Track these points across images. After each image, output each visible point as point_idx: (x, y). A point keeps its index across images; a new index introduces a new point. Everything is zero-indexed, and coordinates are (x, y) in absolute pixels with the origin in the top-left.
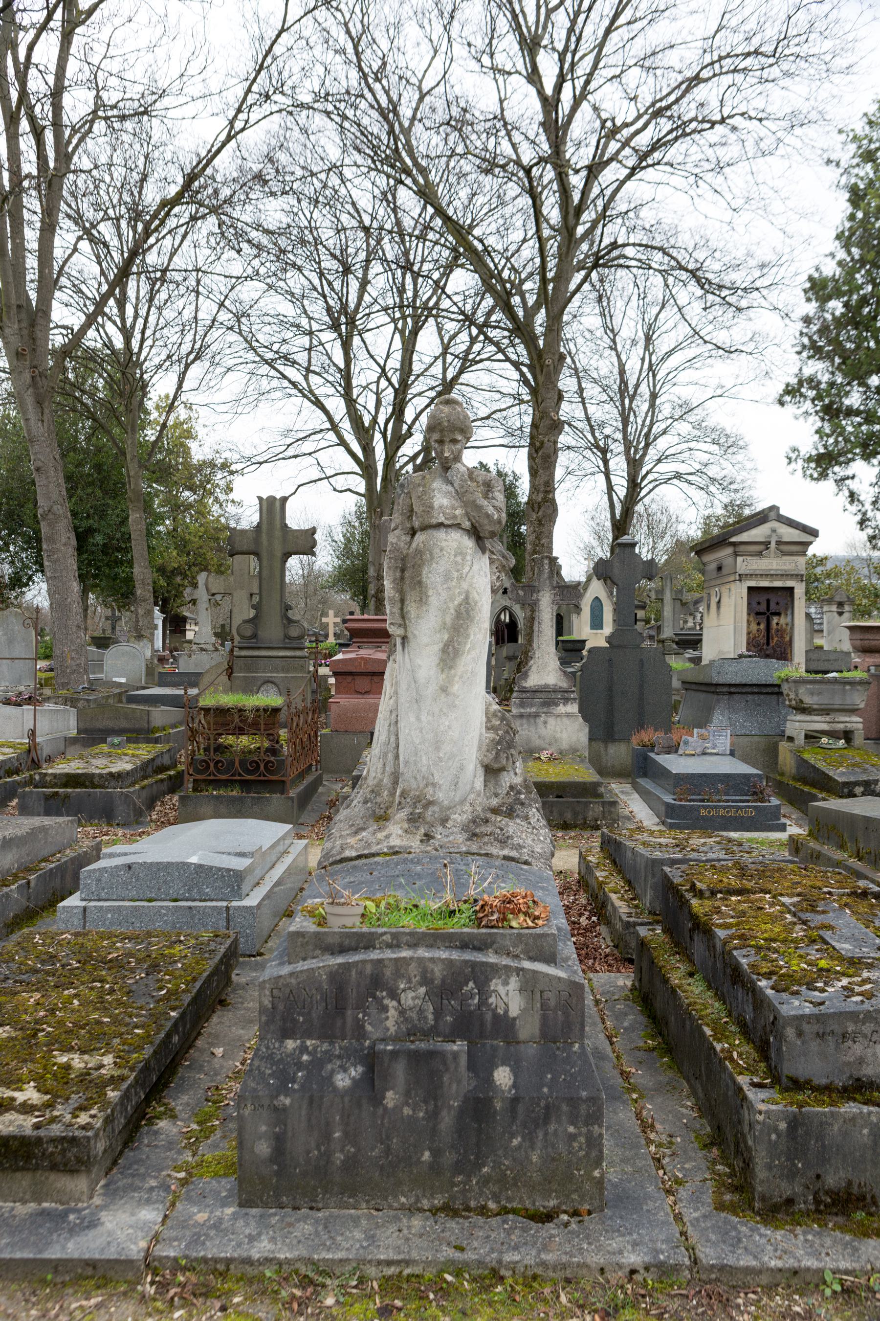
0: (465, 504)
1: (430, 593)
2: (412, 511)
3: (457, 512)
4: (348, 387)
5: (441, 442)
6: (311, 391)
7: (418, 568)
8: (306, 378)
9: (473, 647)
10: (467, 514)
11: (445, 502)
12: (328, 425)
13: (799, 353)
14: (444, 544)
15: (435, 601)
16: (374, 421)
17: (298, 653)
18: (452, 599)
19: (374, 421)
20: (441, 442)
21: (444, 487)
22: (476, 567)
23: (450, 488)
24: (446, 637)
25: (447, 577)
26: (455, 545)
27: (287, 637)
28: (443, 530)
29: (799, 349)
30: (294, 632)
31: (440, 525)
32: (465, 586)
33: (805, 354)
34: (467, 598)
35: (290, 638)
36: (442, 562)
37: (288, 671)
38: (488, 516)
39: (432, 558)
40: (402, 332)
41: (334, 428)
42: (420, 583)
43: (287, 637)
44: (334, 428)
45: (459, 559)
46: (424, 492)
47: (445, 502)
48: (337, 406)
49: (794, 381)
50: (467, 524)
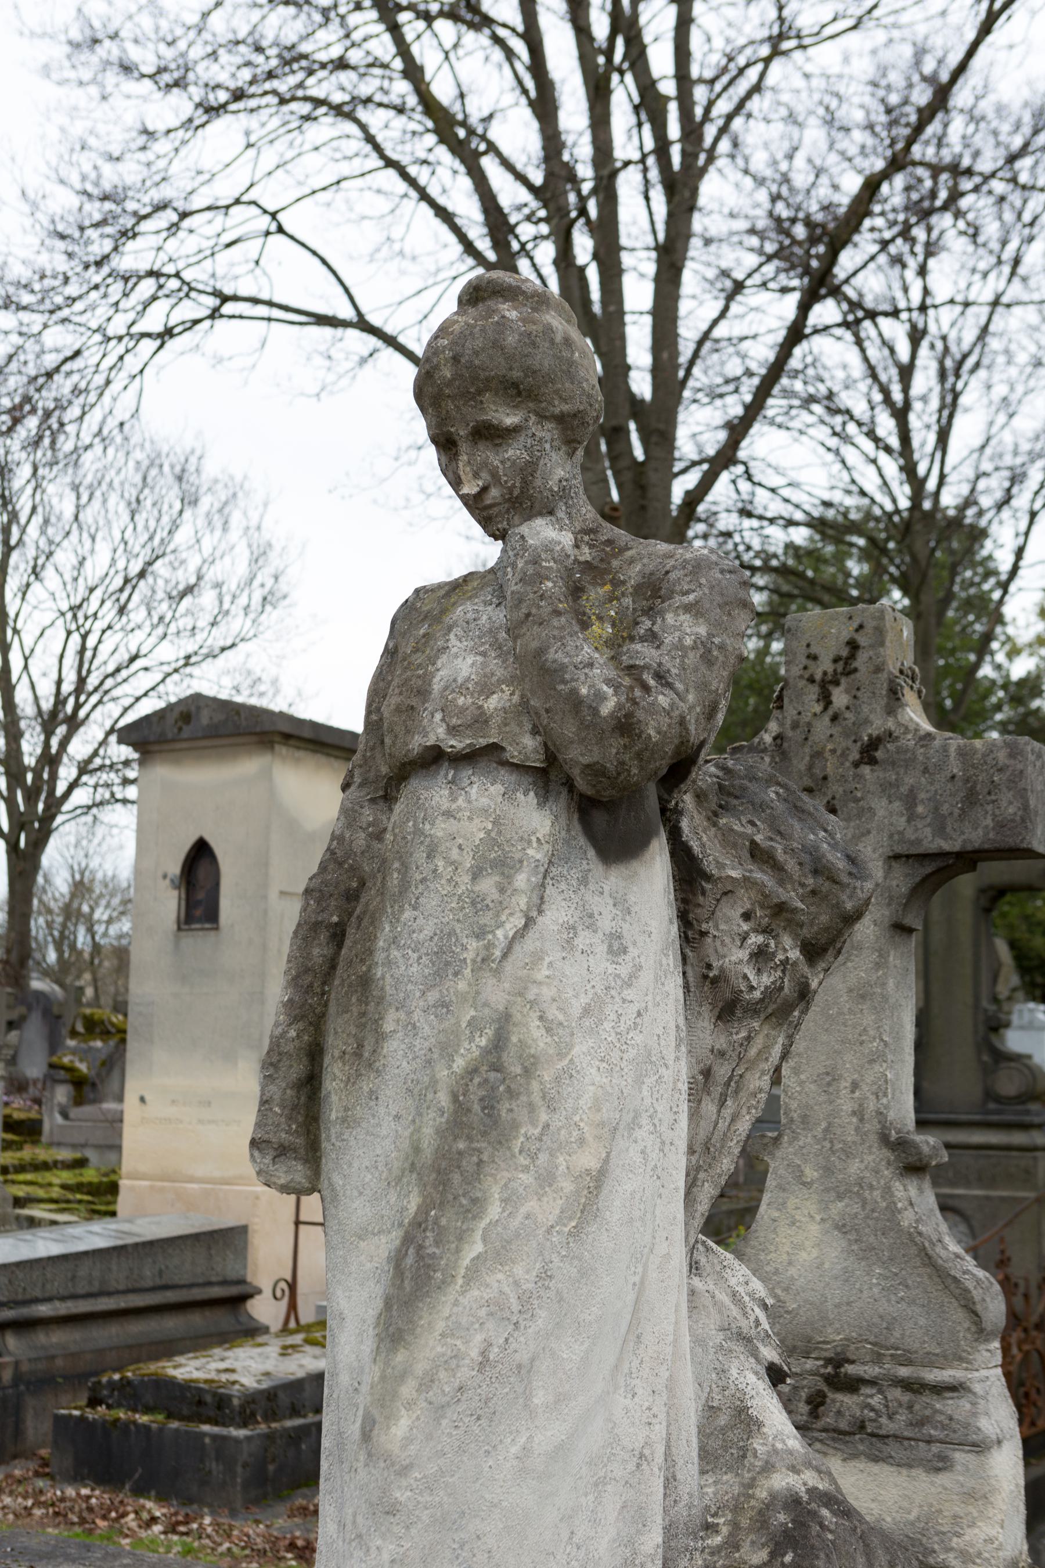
9: (500, 1253)
15: (399, 1054)
17: (1018, 1138)
18: (447, 1049)
22: (557, 914)
24: (413, 1203)
26: (476, 830)
27: (990, 1095)
30: (1008, 1085)
31: (434, 758)
32: (496, 994)
34: (499, 1043)
35: (999, 1099)
36: (430, 902)
37: (991, 1183)
39: (405, 885)
43: (990, 1095)
45: (488, 885)
50: (526, 746)
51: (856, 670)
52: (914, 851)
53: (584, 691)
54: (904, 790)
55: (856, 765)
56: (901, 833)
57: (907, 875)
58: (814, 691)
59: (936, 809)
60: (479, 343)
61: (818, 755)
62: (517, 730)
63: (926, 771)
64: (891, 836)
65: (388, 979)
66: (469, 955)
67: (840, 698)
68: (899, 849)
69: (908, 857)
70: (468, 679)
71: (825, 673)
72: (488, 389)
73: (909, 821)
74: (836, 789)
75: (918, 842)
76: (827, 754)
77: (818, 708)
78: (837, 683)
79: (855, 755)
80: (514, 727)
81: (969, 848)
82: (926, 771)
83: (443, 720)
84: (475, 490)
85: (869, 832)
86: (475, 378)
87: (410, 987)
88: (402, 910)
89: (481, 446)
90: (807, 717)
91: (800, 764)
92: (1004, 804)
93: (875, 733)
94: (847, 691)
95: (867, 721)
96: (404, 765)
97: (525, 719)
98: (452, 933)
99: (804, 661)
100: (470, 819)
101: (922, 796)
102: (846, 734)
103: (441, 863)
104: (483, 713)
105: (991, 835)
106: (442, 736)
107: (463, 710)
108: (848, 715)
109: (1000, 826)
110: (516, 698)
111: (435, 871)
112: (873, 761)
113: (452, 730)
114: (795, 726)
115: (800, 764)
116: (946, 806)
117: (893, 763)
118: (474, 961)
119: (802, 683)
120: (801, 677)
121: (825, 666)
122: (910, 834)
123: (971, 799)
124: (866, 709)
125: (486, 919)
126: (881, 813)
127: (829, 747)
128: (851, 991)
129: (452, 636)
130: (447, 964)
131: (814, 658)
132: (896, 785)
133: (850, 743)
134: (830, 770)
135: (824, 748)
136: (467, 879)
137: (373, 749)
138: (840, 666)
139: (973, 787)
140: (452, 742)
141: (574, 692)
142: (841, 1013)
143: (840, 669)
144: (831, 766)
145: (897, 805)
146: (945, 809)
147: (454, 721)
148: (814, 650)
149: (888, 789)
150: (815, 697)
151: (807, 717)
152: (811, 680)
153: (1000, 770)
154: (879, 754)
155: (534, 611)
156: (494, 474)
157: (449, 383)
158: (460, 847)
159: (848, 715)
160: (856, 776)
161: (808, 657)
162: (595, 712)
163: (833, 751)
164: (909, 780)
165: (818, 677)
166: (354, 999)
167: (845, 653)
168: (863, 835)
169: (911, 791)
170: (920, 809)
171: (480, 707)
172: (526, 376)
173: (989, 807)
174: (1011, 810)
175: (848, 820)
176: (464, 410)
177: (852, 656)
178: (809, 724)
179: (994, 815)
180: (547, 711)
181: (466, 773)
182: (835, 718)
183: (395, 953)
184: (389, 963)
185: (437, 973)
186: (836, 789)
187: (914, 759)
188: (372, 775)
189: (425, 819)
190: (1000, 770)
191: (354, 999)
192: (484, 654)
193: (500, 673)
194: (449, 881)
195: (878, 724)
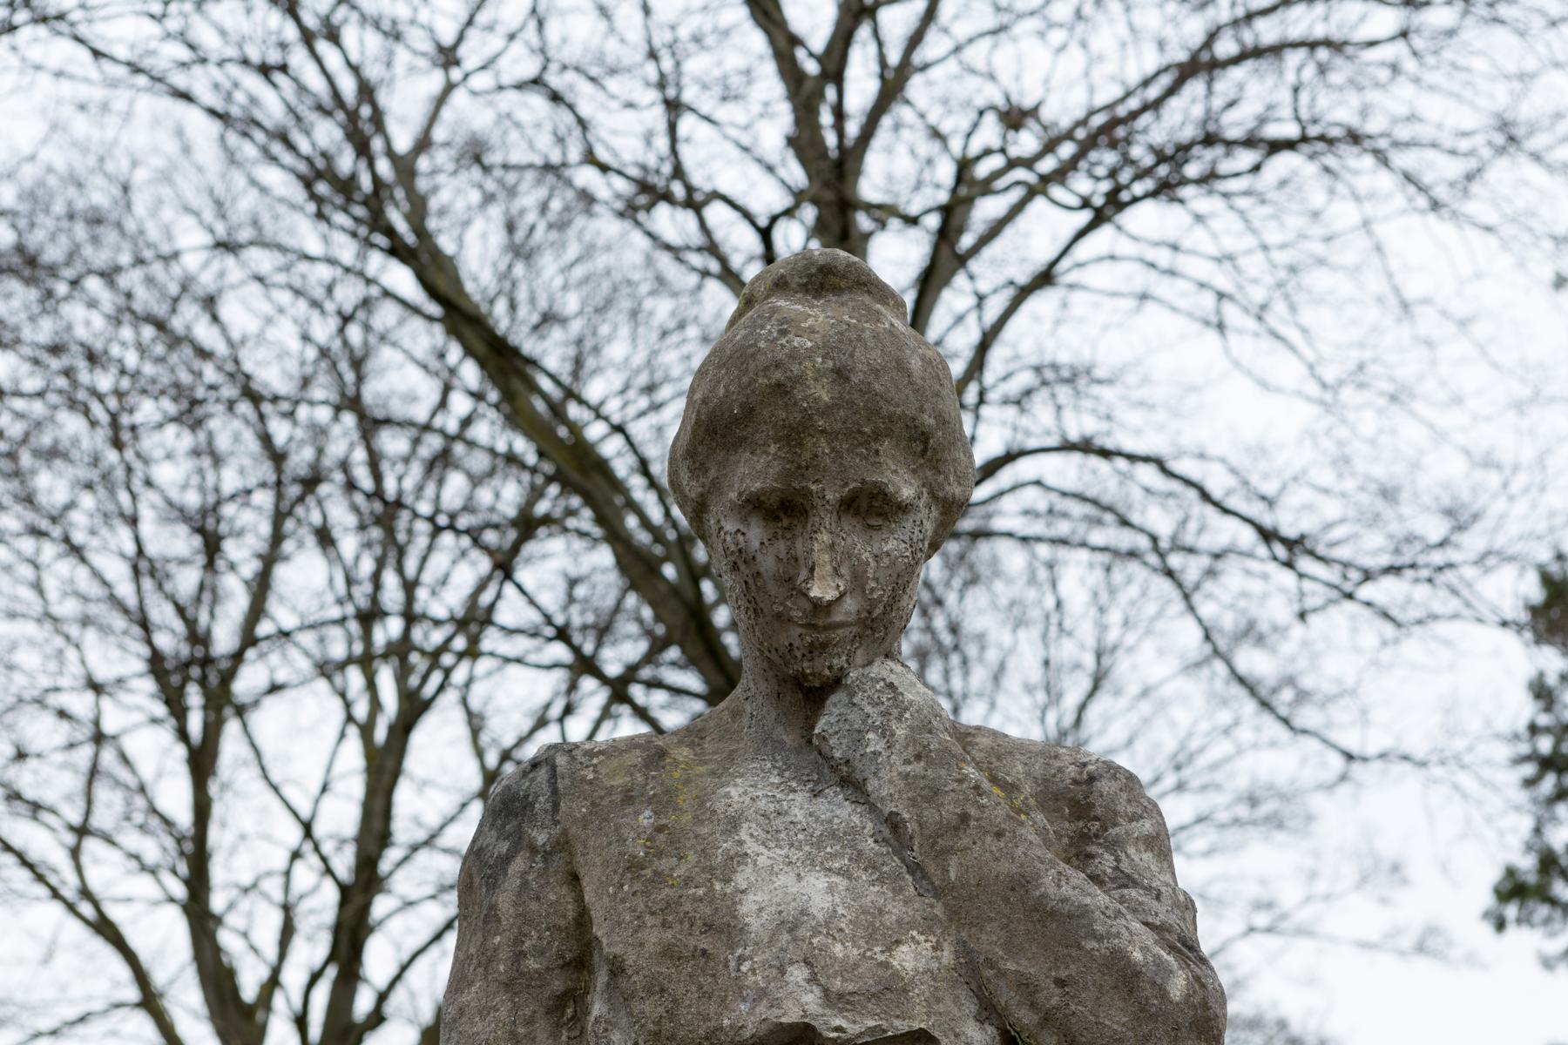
0: (956, 906)
2: (580, 954)
3: (907, 958)
4: (198, 882)
5: (784, 510)
6: (86, 893)
8: (75, 853)
10: (973, 974)
11: (818, 892)
12: (132, 993)
13: (1530, 783)
16: (273, 982)
19: (273, 982)
20: (784, 510)
21: (799, 806)
23: (840, 810)
29: (1529, 769)
33: (1549, 783)
38: (1127, 978)
40: (366, 730)
41: (151, 1002)
44: (151, 1002)
46: (667, 839)
47: (818, 892)
48: (163, 938)
49: (1527, 864)
53: (1137, 956)
60: (876, 356)
62: (955, 1011)
70: (833, 914)
72: (889, 434)
80: (948, 1005)
83: (813, 979)
84: (830, 595)
86: (873, 412)
89: (848, 523)
97: (963, 993)
104: (896, 975)
107: (848, 969)
110: (947, 956)
113: (832, 999)
129: (743, 835)
137: (529, 1022)
140: (837, 1022)
141: (1119, 956)
147: (837, 984)
155: (973, 812)
156: (858, 578)
157: (827, 411)
162: (1164, 995)
171: (885, 965)
172: (938, 428)
176: (847, 460)
180: (1060, 983)
192: (839, 872)
193: (895, 910)
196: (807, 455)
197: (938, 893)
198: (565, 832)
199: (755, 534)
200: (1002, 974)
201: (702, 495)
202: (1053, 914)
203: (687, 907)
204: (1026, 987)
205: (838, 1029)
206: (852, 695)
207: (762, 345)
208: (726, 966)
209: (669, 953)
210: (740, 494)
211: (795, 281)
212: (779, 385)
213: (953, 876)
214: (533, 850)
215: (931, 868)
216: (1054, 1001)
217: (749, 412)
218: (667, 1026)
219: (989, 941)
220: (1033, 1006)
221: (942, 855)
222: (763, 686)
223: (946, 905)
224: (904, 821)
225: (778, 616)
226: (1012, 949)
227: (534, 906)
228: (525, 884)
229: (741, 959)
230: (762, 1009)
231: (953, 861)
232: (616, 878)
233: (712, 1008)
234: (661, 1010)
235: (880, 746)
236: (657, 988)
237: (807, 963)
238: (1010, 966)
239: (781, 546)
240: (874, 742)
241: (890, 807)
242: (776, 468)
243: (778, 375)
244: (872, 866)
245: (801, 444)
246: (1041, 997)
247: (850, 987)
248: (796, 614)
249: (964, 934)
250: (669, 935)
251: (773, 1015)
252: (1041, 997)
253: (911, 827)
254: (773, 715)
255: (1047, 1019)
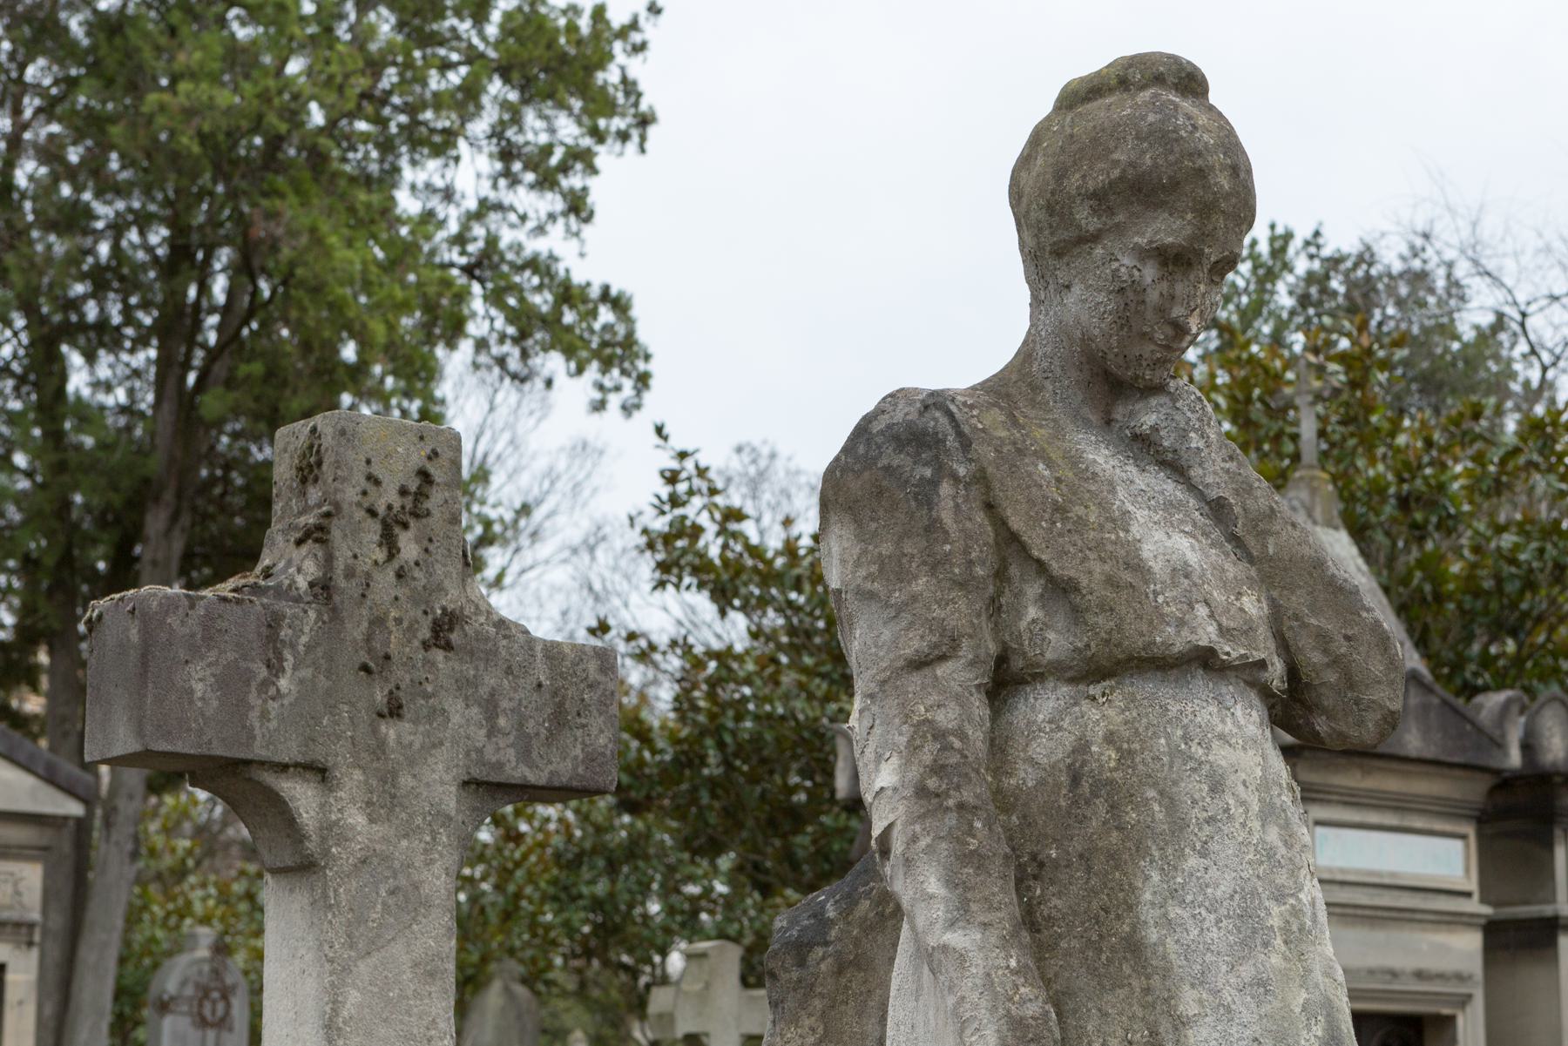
1: (1189, 1001)
7: (1111, 870)
14: (1222, 756)
21: (1140, 481)
25: (1251, 934)
28: (1200, 683)
36: (1225, 850)
39: (1179, 826)
42: (1134, 947)
50: (1276, 672)
51: (428, 514)
52: (495, 778)
54: (483, 691)
55: (426, 646)
56: (480, 751)
57: (474, 809)
58: (373, 531)
59: (521, 725)
61: (378, 622)
63: (509, 671)
64: (467, 754)
65: (1171, 945)
66: (1275, 922)
67: (409, 548)
68: (476, 772)
69: (488, 784)
71: (390, 507)
73: (489, 735)
74: (401, 675)
75: (500, 766)
76: (391, 624)
77: (380, 555)
78: (405, 526)
79: (425, 633)
81: (556, 784)
82: (509, 671)
83: (1212, 616)
85: (441, 744)
87: (1209, 957)
88: (1181, 855)
90: (364, 565)
91: (356, 630)
92: (594, 732)
93: (450, 607)
94: (418, 540)
95: (440, 588)
96: (1130, 659)
98: (1254, 893)
99: (364, 483)
100: (1244, 749)
101: (505, 704)
102: (415, 602)
103: (1231, 802)
105: (580, 770)
106: (1214, 637)
108: (417, 573)
109: (591, 759)
111: (1227, 810)
112: (448, 647)
113: (1223, 631)
114: (350, 573)
115: (356, 630)
116: (531, 723)
117: (472, 653)
118: (1286, 930)
119: (360, 514)
120: (359, 504)
121: (388, 497)
122: (490, 755)
123: (559, 719)
124: (439, 570)
125: (1282, 878)
126: (456, 719)
127: (393, 614)
128: (416, 965)
130: (1254, 931)
131: (374, 480)
132: (474, 683)
133: (420, 613)
134: (393, 649)
135: (386, 613)
136: (1256, 825)
138: (409, 502)
139: (561, 705)
140: (1227, 649)
142: (403, 997)
143: (409, 506)
144: (395, 642)
145: (475, 711)
146: (530, 726)
148: (377, 470)
149: (465, 686)
150: (376, 538)
151: (364, 565)
152: (372, 513)
153: (590, 686)
154: (455, 637)
157: (1227, 196)
158: (1244, 783)
159: (417, 573)
160: (426, 661)
161: (369, 477)
163: (399, 621)
164: (490, 681)
165: (381, 510)
166: (1126, 969)
167: (413, 486)
168: (434, 746)
169: (492, 695)
170: (502, 722)
173: (579, 733)
174: (602, 741)
175: (416, 722)
177: (421, 495)
178: (368, 575)
179: (583, 743)
180: (1347, 638)
181: (1228, 690)
182: (400, 575)
183: (1175, 911)
184: (1168, 923)
185: (1243, 943)
186: (401, 675)
187: (496, 653)
188: (982, 652)
189: (1187, 738)
190: (590, 686)
191: (1126, 969)
194: (1243, 825)
195: (451, 598)
196: (1210, 227)
197: (1251, 560)
198: (983, 470)
199: (1149, 273)
200: (1305, 625)
201: (1100, 230)
202: (1341, 589)
203: (1109, 547)
204: (1323, 639)
205: (1228, 654)
206: (1174, 400)
207: (1183, 133)
208: (1147, 596)
209: (1111, 582)
210: (1151, 242)
211: (1171, 80)
212: (1201, 170)
213: (1271, 551)
214: (956, 478)
215: (1251, 542)
216: (1343, 650)
217: (1175, 185)
218: (1116, 636)
219: (1297, 601)
220: (1325, 651)
221: (1262, 535)
222: (1074, 374)
223: (1259, 571)
224: (1230, 505)
225: (1145, 334)
226: (1315, 610)
227: (968, 525)
228: (957, 506)
229: (1156, 593)
230: (1185, 632)
231: (1271, 540)
232: (1047, 516)
233: (1145, 628)
234: (1112, 624)
235: (1201, 444)
236: (1106, 608)
237: (1207, 603)
238: (1313, 621)
239: (1165, 284)
240: (1195, 441)
241: (1213, 494)
242: (1189, 231)
243: (1200, 162)
244: (1206, 534)
245: (1208, 218)
246: (1333, 646)
247: (1232, 625)
248: (1159, 336)
249: (1275, 594)
250: (1107, 567)
251: (1193, 638)
252: (1333, 646)
253: (1237, 510)
254: (1080, 397)
255: (1336, 662)
